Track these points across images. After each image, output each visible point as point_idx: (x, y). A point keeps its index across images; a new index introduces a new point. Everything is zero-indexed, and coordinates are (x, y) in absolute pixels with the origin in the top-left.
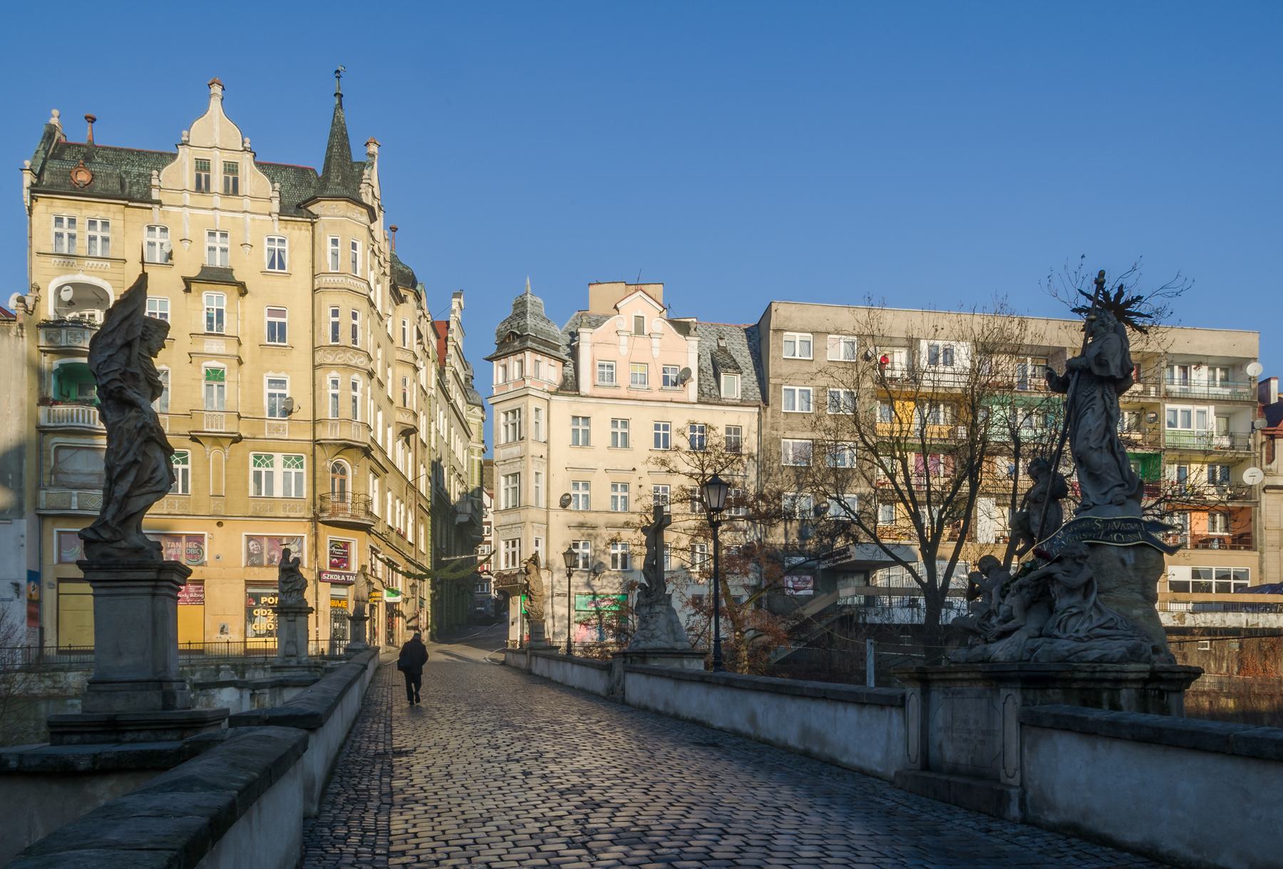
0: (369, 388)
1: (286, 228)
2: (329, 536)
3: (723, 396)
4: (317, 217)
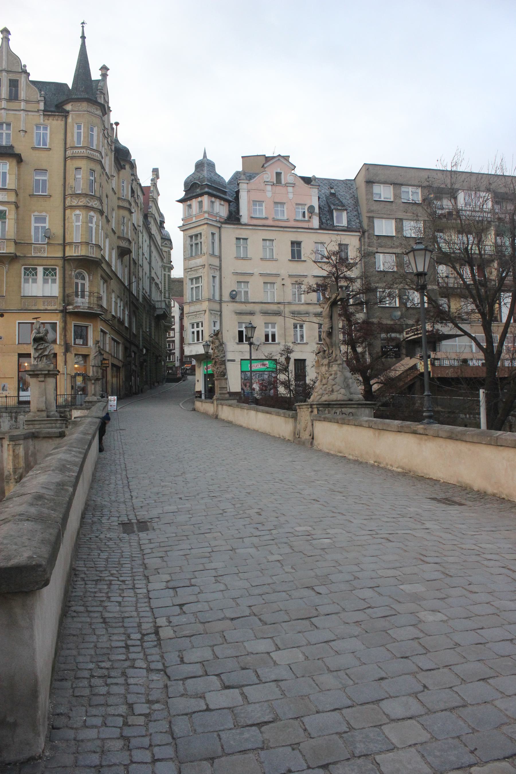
0: (100, 222)
1: (48, 120)
2: (73, 322)
3: (335, 224)
4: (68, 112)
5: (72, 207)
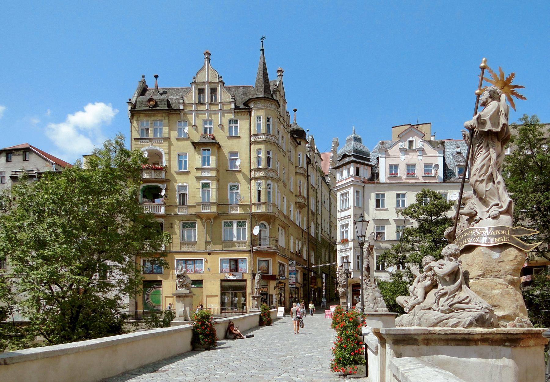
1: (238, 115)
5: (256, 179)
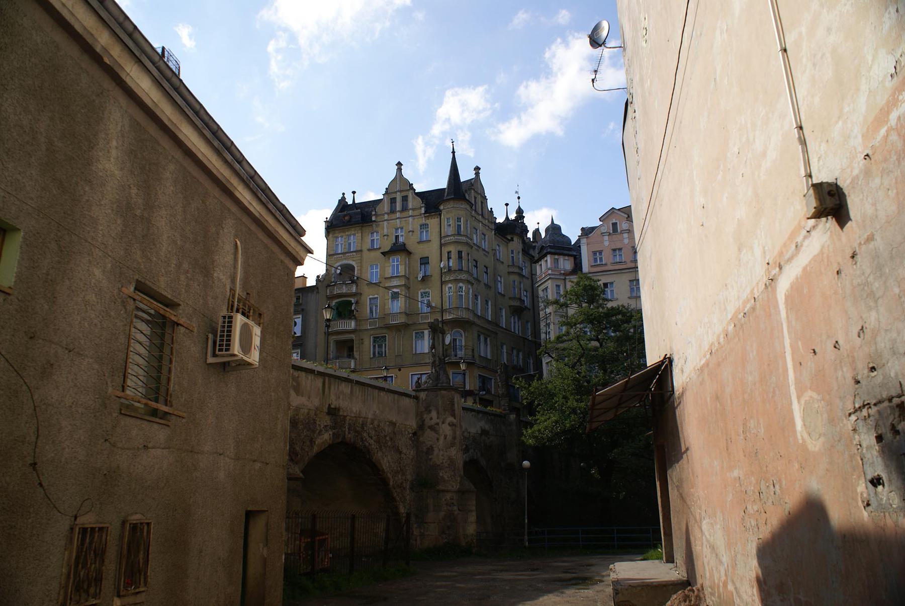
1: (428, 219)
